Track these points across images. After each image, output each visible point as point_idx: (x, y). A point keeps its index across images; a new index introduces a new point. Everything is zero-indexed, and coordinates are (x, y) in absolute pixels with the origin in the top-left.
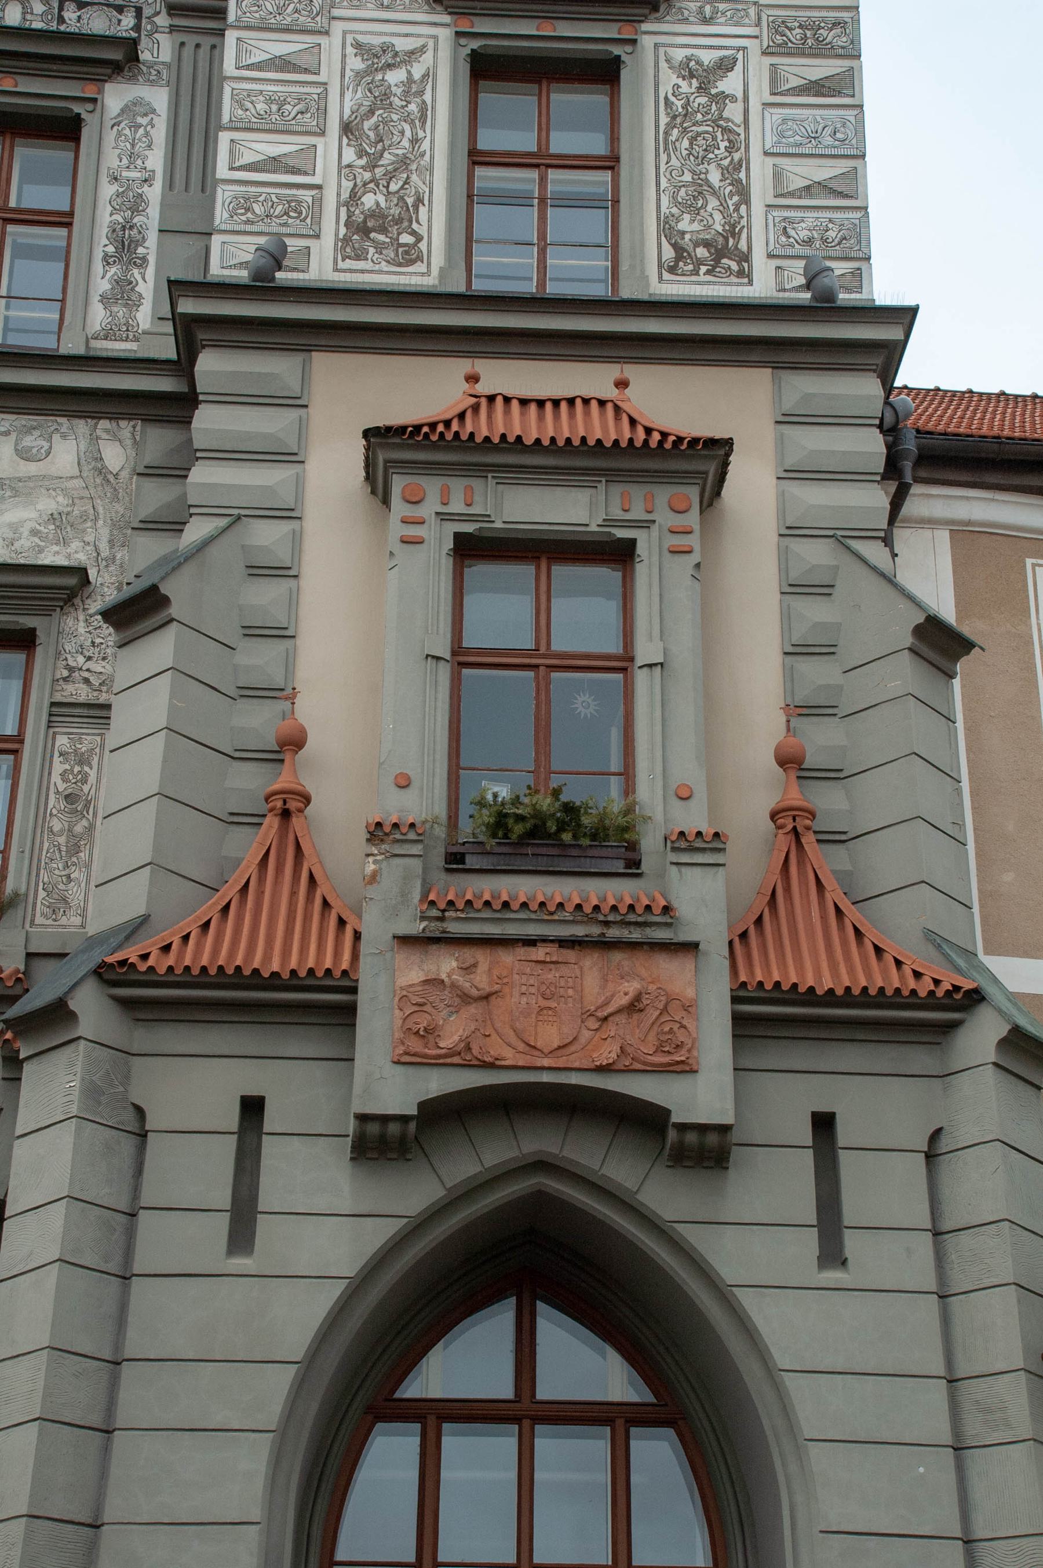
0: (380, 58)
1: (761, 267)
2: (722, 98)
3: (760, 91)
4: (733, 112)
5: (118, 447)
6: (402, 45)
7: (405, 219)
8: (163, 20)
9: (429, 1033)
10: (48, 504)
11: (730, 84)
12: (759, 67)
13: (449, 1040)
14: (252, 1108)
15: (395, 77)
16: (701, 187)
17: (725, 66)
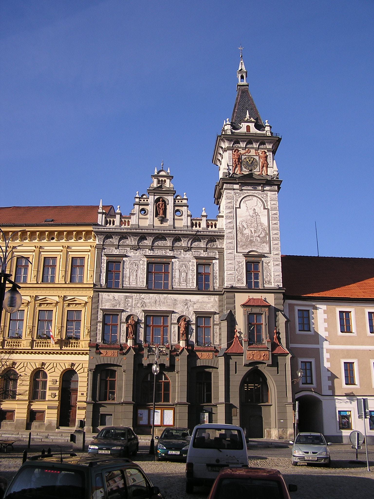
0: (239, 262)
1: (273, 283)
2: (269, 266)
3: (272, 265)
4: (270, 267)
5: (217, 298)
6: (241, 261)
7: (242, 279)
8: (218, 253)
9: (250, 358)
10: (212, 304)
11: (269, 264)
12: (272, 262)
13: (251, 358)
14: (236, 362)
15: (240, 264)
16: (267, 275)
17: (269, 262)
